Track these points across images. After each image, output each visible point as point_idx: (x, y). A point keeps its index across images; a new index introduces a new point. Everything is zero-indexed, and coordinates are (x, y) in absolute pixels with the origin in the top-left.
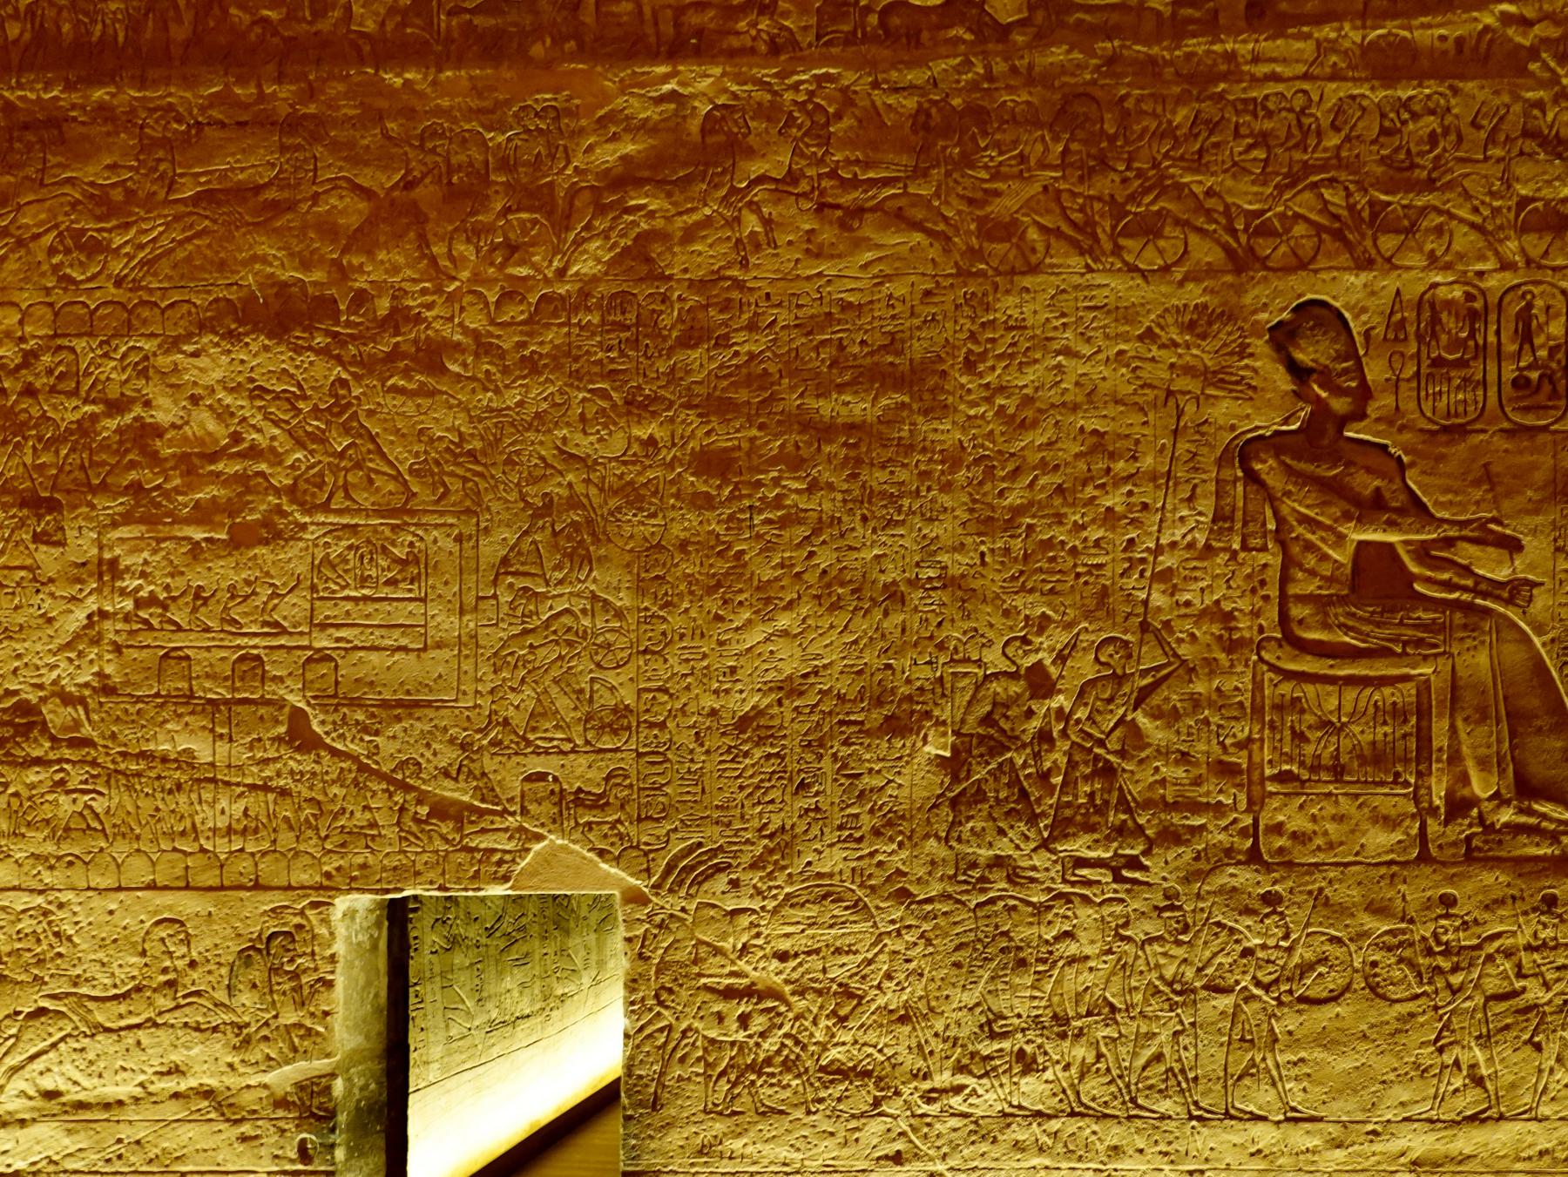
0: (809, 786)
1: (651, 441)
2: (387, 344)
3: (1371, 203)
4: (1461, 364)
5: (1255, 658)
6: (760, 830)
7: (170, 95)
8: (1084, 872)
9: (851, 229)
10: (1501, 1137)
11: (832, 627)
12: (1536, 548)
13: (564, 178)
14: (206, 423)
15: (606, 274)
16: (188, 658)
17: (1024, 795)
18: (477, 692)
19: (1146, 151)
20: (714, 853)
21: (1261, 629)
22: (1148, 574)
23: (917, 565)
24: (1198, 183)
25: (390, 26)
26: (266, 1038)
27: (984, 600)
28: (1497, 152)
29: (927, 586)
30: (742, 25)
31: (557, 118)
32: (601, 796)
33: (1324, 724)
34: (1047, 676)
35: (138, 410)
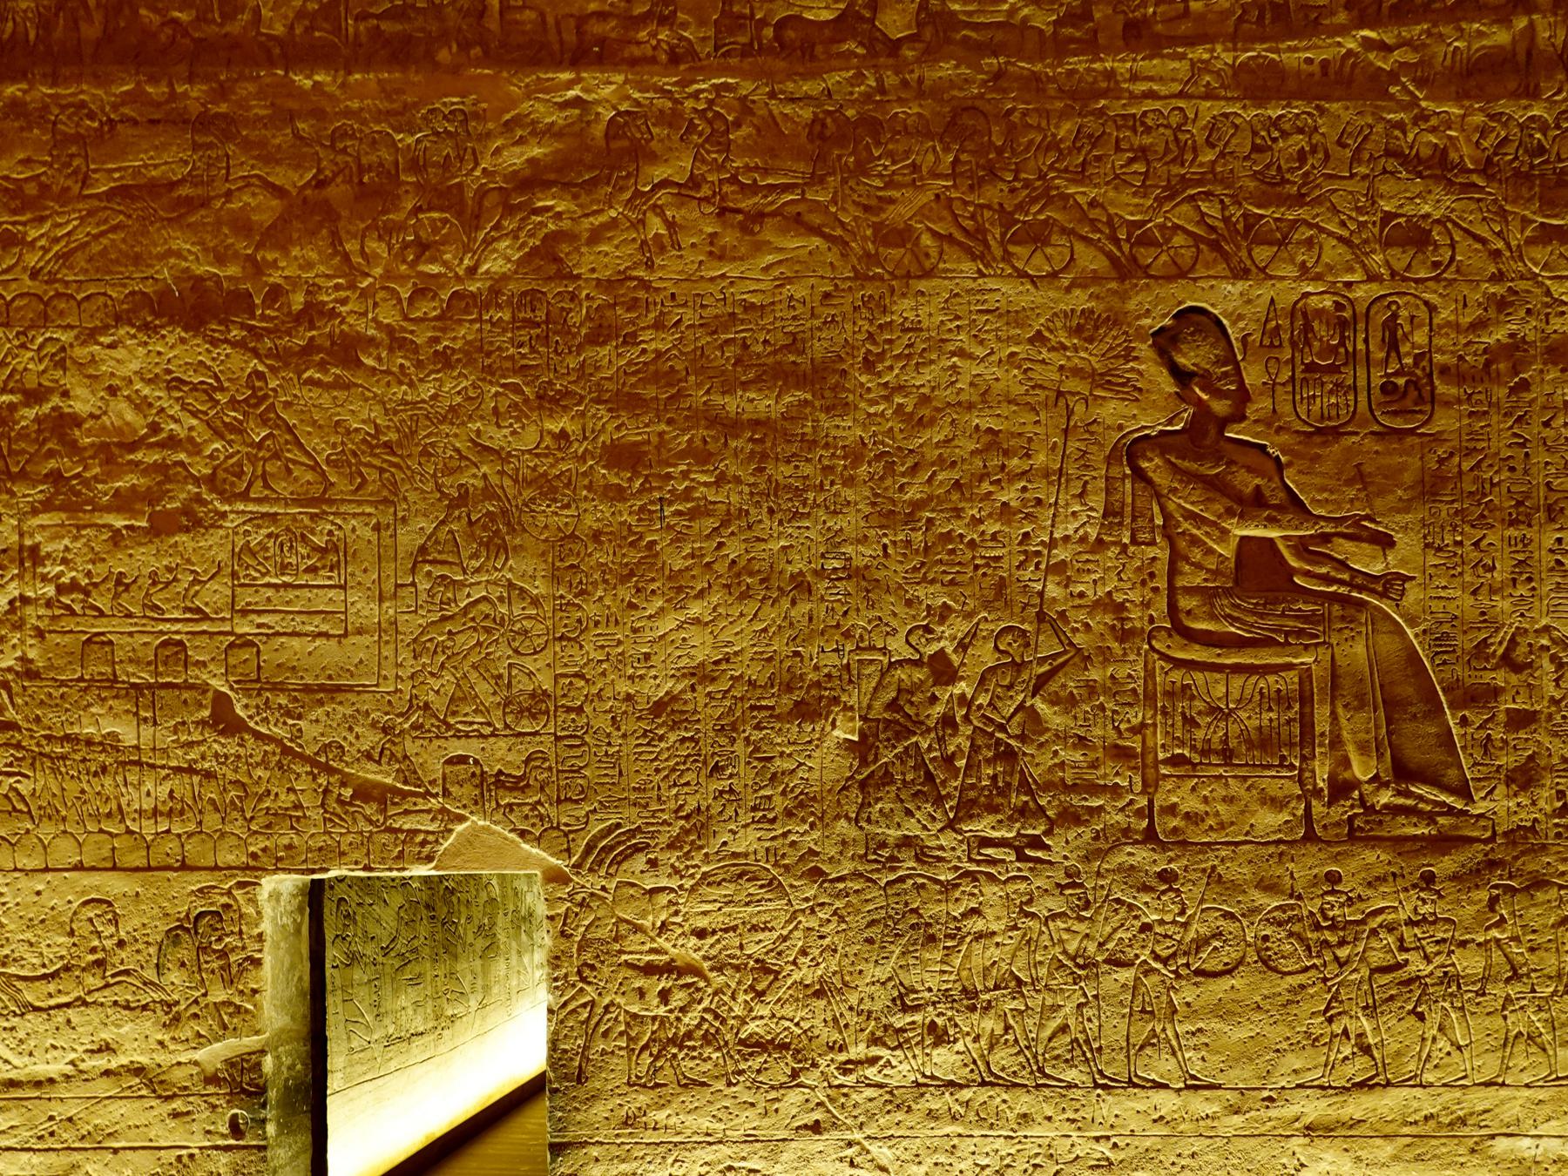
0: (723, 768)
1: (563, 435)
2: (302, 338)
3: (1245, 216)
4: (1333, 369)
6: (676, 811)
7: (82, 92)
8: (990, 851)
9: (752, 233)
10: (1387, 1103)
11: (742, 615)
12: (1407, 544)
13: (472, 180)
14: (123, 413)
15: (516, 272)
16: (110, 643)
17: (930, 777)
18: (397, 676)
19: (1032, 163)
20: (632, 833)
21: (1152, 620)
22: (1043, 566)
23: (823, 556)
24: (1082, 193)
25: (298, 31)
26: (196, 1016)
27: (888, 591)
28: (1363, 170)
29: (832, 577)
30: (642, 35)
31: (466, 121)
32: (521, 778)
33: (1213, 710)
34: (949, 663)
35: (55, 400)
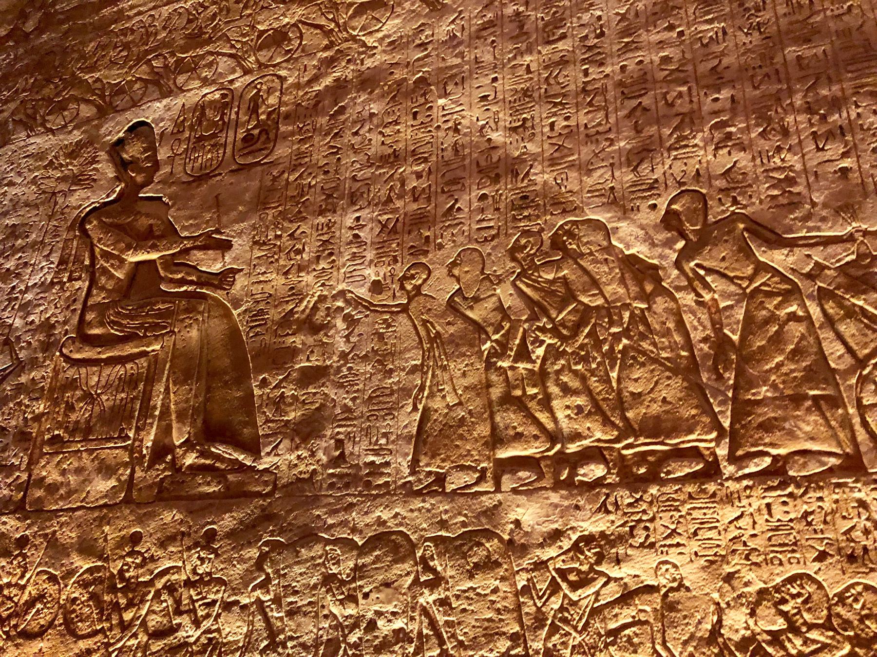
5: (58, 354)
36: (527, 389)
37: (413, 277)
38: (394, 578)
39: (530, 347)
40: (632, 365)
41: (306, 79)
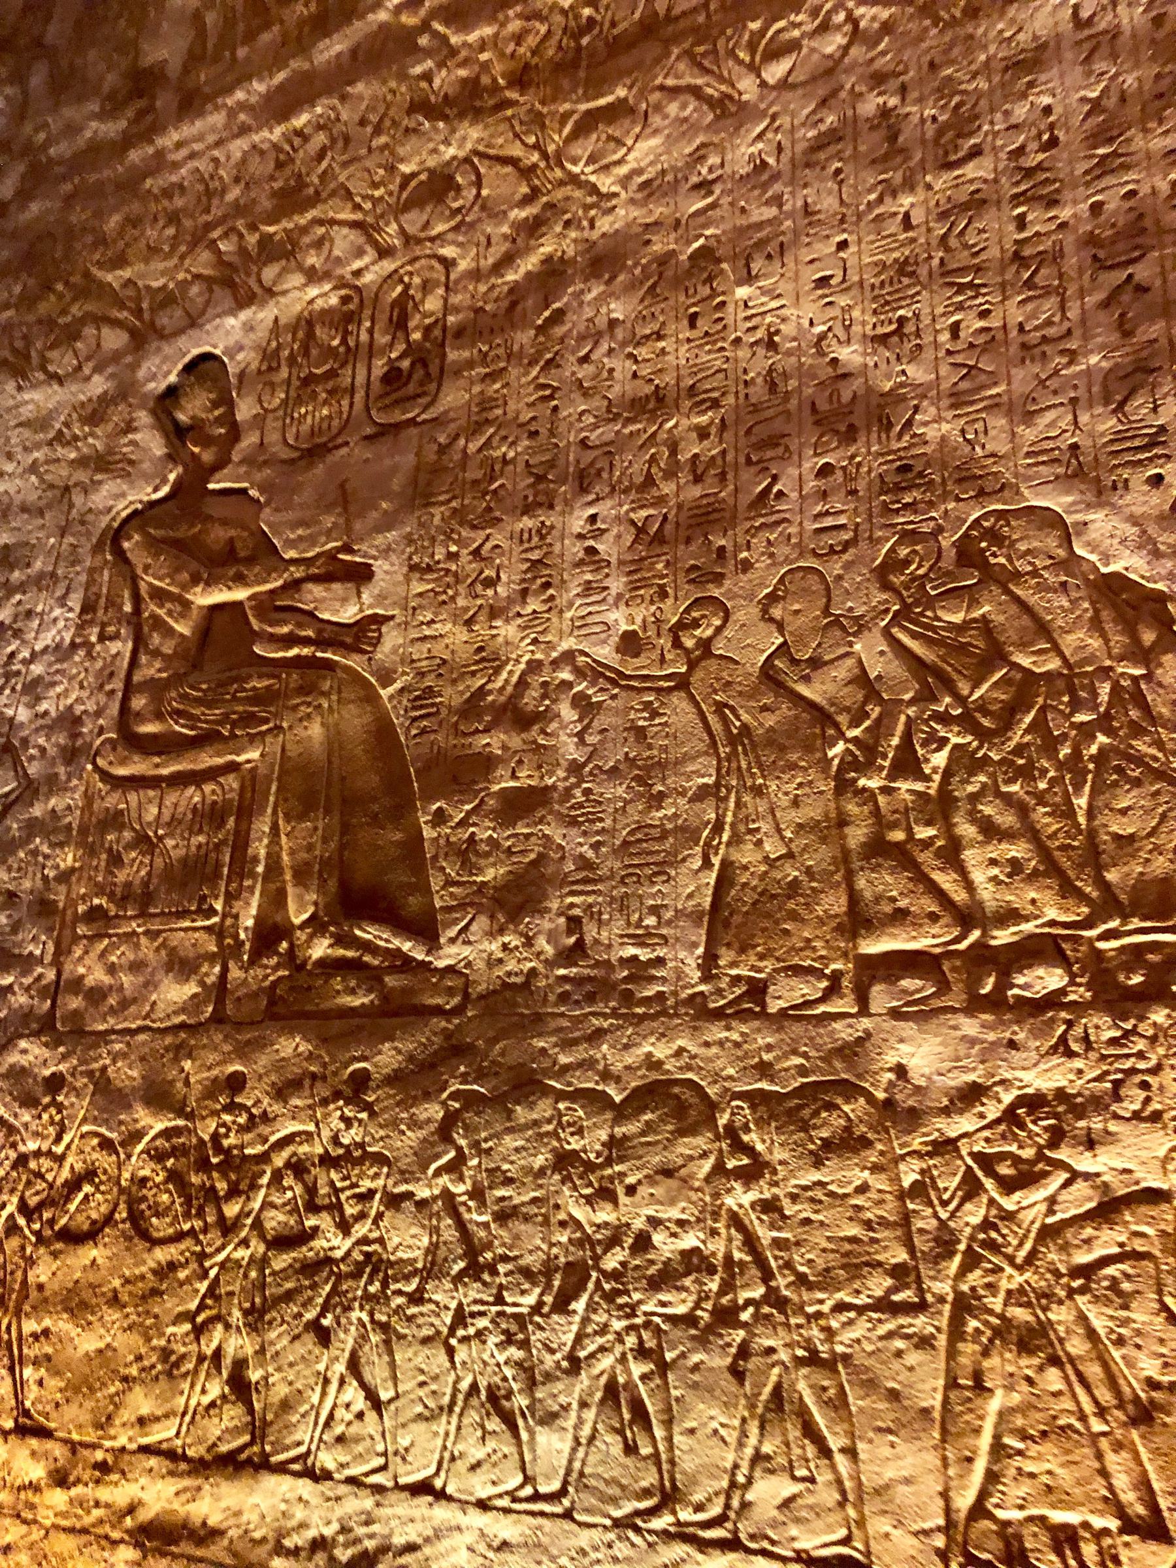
5: (89, 767)
36: (916, 829)
37: (696, 624)
38: (680, 1161)
39: (920, 752)
40: (1115, 784)
41: (491, 261)
